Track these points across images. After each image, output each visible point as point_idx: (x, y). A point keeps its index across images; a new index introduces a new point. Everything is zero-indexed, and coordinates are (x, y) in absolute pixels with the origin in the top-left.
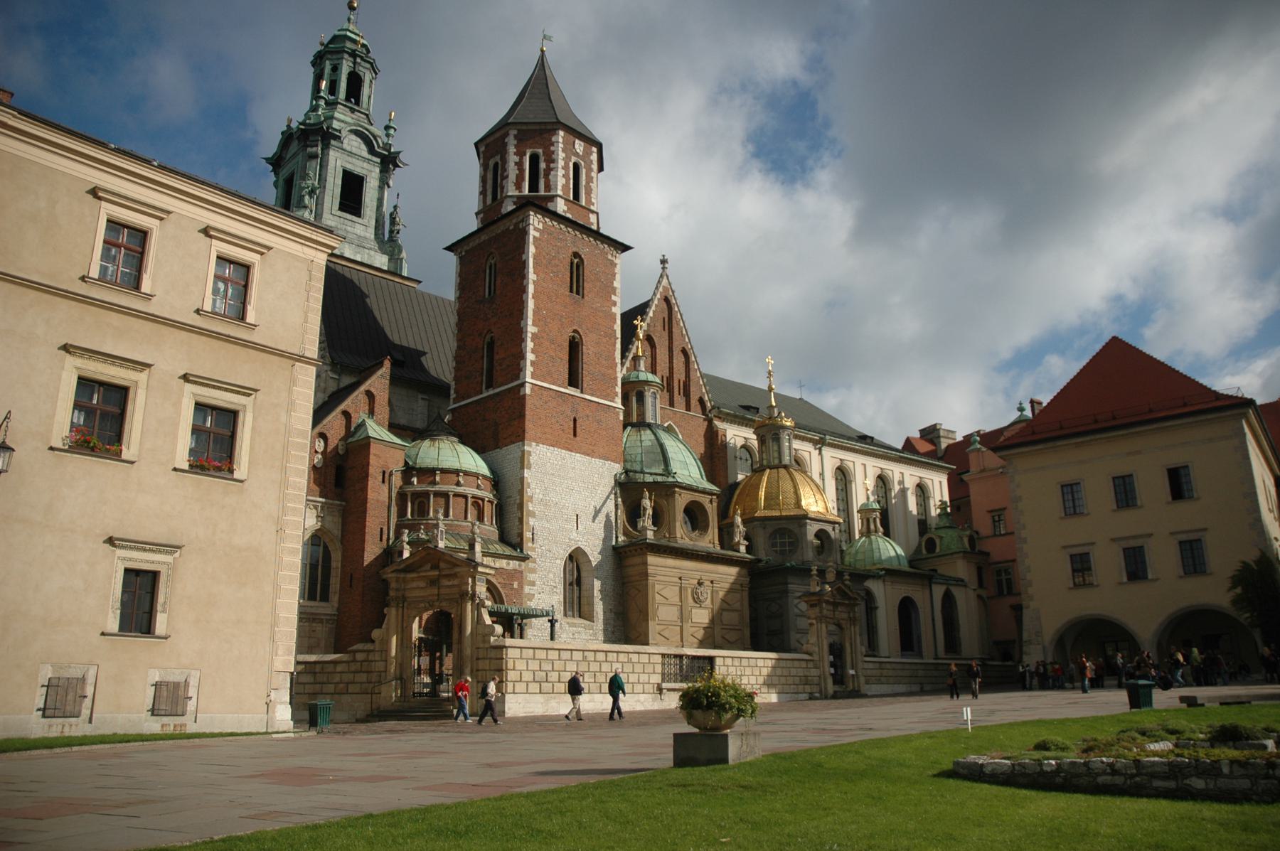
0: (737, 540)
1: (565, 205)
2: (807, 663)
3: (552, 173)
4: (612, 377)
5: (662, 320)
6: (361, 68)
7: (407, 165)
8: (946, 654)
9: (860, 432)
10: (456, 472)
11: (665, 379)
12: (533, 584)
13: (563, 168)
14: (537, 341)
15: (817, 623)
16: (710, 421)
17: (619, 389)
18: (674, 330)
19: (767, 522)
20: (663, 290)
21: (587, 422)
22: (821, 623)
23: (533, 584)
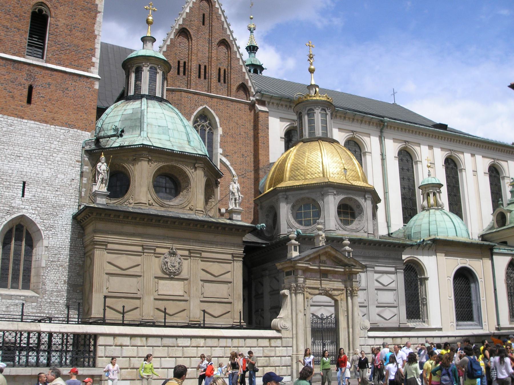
4: (88, 48)
5: (202, 16)
8: (510, 324)
9: (435, 123)
11: (203, 67)
15: (291, 294)
17: (96, 60)
18: (213, 24)
19: (288, 193)
22: (296, 294)
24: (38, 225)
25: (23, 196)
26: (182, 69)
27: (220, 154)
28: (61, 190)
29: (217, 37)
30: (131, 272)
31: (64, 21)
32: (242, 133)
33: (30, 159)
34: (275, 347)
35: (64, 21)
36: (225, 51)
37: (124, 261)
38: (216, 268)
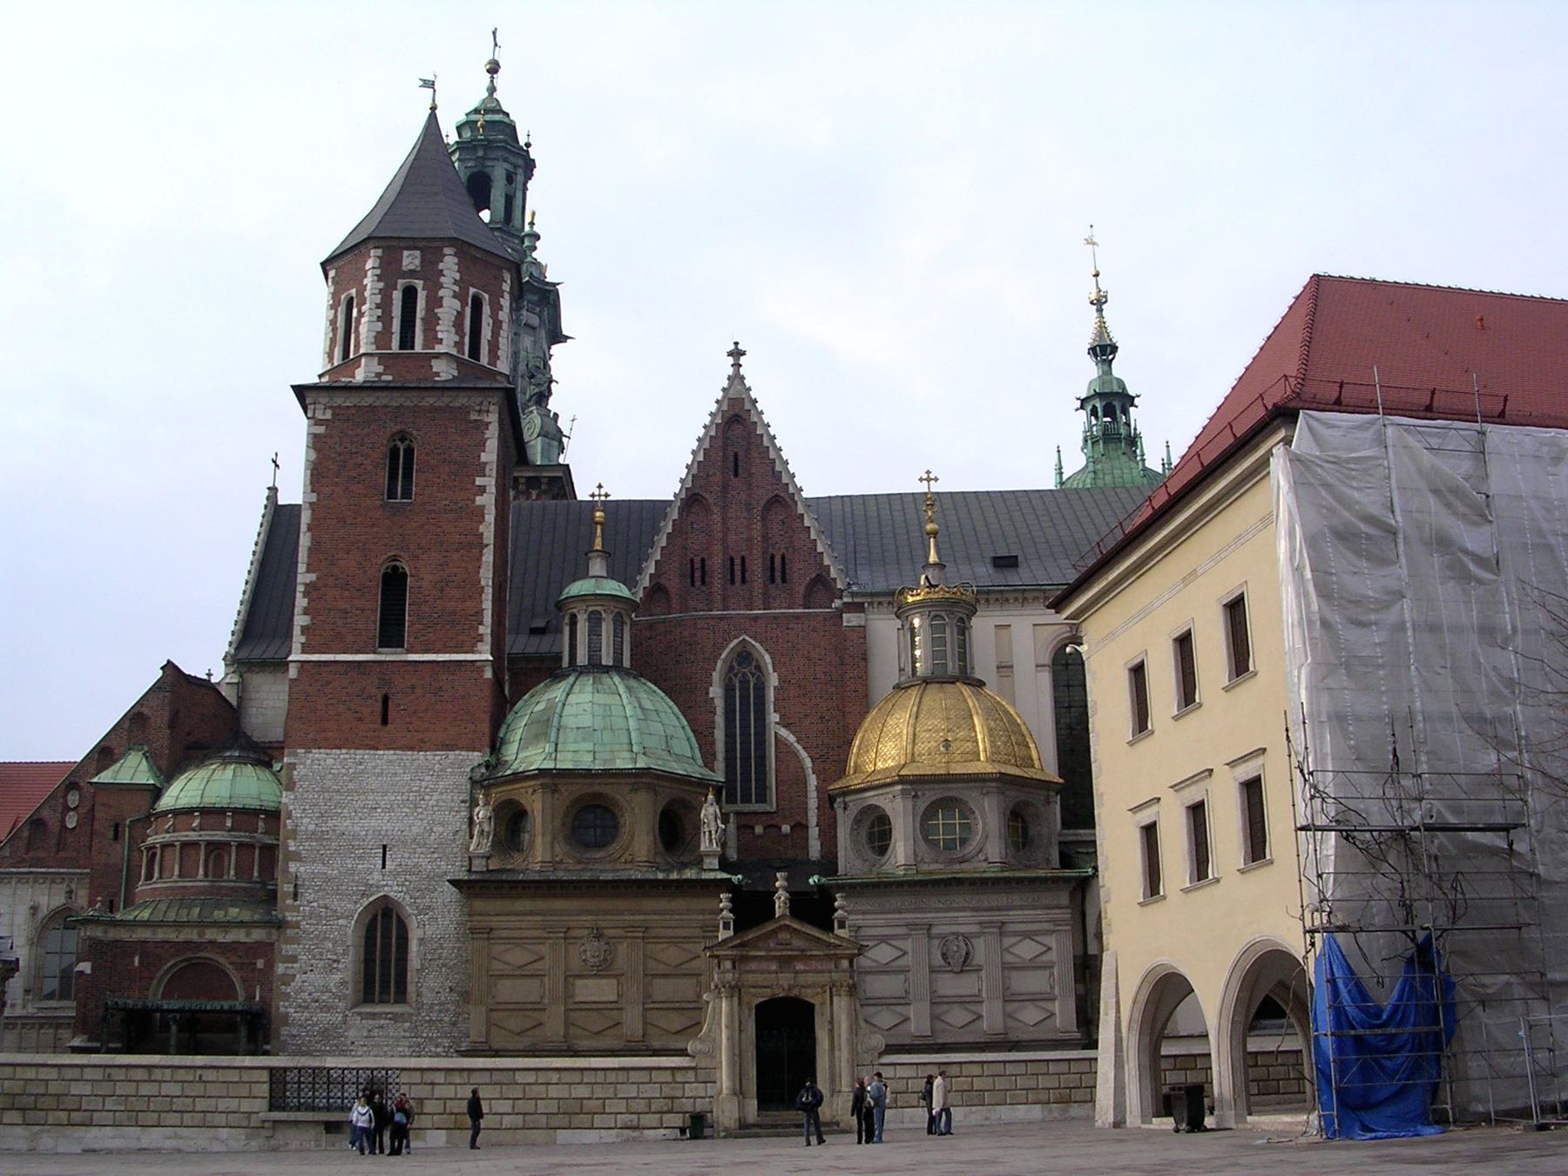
0: (702, 848)
1: (379, 364)
2: (673, 1075)
3: (363, 320)
4: (472, 613)
5: (731, 458)
6: (489, 163)
7: (559, 284)
10: (188, 812)
11: (738, 561)
12: (294, 959)
13: (378, 306)
14: (315, 594)
16: (839, 614)
17: (486, 630)
19: (847, 799)
20: (729, 406)
21: (413, 696)
23: (293, 959)
24: (407, 908)
25: (384, 867)
26: (698, 574)
27: (776, 723)
28: (439, 850)
29: (763, 495)
30: (531, 969)
31: (430, 577)
32: (818, 676)
33: (391, 810)
34: (684, 1083)
35: (430, 577)
36: (781, 517)
37: (517, 956)
38: (672, 955)
